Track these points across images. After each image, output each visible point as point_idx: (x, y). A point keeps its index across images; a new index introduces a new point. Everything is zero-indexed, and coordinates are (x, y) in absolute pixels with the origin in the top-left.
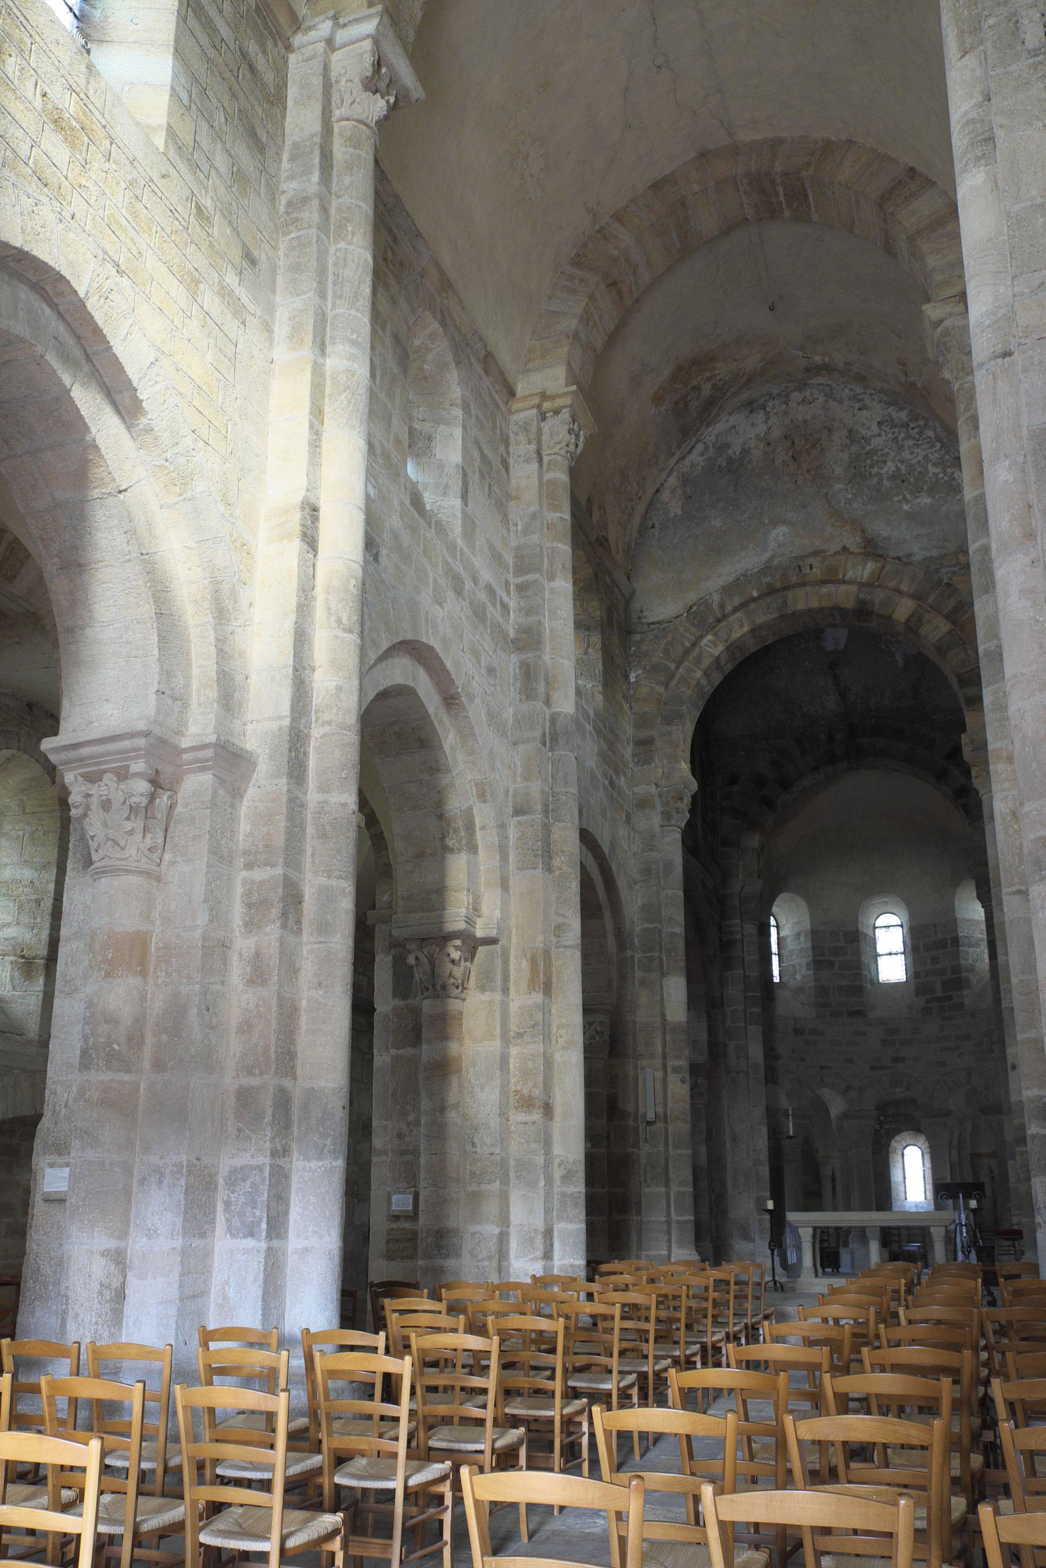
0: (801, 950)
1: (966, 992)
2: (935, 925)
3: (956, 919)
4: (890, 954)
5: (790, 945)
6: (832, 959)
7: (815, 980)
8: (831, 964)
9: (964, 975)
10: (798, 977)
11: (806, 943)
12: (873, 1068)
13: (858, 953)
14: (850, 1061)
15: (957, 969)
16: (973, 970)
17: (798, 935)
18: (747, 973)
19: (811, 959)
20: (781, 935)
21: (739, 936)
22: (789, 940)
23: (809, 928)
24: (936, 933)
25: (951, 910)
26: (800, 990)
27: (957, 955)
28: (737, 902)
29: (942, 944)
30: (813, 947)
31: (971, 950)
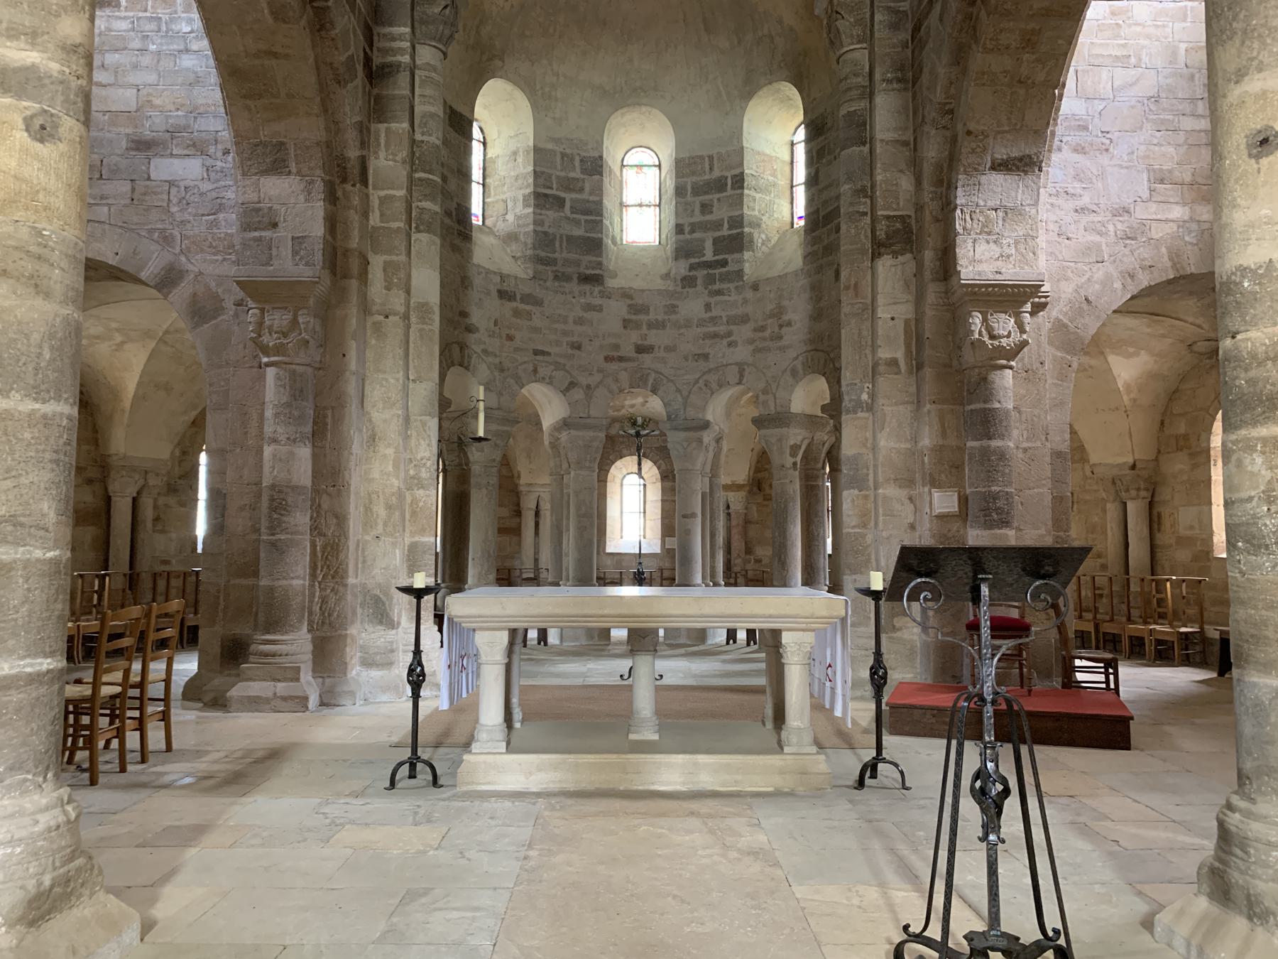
0: (517, 178)
1: (747, 255)
2: (711, 158)
3: (742, 148)
4: (640, 205)
5: (501, 169)
6: (562, 195)
7: (535, 223)
8: (560, 202)
9: (746, 230)
10: (510, 217)
11: (525, 167)
12: (607, 359)
13: (599, 190)
14: (578, 347)
15: (737, 222)
16: (759, 225)
17: (515, 153)
18: (418, 137)
19: (530, 190)
20: (489, 156)
21: (406, 59)
22: (500, 162)
23: (531, 144)
25: (737, 133)
26: (511, 237)
27: (739, 201)
29: (720, 185)
30: (535, 172)
31: (758, 196)
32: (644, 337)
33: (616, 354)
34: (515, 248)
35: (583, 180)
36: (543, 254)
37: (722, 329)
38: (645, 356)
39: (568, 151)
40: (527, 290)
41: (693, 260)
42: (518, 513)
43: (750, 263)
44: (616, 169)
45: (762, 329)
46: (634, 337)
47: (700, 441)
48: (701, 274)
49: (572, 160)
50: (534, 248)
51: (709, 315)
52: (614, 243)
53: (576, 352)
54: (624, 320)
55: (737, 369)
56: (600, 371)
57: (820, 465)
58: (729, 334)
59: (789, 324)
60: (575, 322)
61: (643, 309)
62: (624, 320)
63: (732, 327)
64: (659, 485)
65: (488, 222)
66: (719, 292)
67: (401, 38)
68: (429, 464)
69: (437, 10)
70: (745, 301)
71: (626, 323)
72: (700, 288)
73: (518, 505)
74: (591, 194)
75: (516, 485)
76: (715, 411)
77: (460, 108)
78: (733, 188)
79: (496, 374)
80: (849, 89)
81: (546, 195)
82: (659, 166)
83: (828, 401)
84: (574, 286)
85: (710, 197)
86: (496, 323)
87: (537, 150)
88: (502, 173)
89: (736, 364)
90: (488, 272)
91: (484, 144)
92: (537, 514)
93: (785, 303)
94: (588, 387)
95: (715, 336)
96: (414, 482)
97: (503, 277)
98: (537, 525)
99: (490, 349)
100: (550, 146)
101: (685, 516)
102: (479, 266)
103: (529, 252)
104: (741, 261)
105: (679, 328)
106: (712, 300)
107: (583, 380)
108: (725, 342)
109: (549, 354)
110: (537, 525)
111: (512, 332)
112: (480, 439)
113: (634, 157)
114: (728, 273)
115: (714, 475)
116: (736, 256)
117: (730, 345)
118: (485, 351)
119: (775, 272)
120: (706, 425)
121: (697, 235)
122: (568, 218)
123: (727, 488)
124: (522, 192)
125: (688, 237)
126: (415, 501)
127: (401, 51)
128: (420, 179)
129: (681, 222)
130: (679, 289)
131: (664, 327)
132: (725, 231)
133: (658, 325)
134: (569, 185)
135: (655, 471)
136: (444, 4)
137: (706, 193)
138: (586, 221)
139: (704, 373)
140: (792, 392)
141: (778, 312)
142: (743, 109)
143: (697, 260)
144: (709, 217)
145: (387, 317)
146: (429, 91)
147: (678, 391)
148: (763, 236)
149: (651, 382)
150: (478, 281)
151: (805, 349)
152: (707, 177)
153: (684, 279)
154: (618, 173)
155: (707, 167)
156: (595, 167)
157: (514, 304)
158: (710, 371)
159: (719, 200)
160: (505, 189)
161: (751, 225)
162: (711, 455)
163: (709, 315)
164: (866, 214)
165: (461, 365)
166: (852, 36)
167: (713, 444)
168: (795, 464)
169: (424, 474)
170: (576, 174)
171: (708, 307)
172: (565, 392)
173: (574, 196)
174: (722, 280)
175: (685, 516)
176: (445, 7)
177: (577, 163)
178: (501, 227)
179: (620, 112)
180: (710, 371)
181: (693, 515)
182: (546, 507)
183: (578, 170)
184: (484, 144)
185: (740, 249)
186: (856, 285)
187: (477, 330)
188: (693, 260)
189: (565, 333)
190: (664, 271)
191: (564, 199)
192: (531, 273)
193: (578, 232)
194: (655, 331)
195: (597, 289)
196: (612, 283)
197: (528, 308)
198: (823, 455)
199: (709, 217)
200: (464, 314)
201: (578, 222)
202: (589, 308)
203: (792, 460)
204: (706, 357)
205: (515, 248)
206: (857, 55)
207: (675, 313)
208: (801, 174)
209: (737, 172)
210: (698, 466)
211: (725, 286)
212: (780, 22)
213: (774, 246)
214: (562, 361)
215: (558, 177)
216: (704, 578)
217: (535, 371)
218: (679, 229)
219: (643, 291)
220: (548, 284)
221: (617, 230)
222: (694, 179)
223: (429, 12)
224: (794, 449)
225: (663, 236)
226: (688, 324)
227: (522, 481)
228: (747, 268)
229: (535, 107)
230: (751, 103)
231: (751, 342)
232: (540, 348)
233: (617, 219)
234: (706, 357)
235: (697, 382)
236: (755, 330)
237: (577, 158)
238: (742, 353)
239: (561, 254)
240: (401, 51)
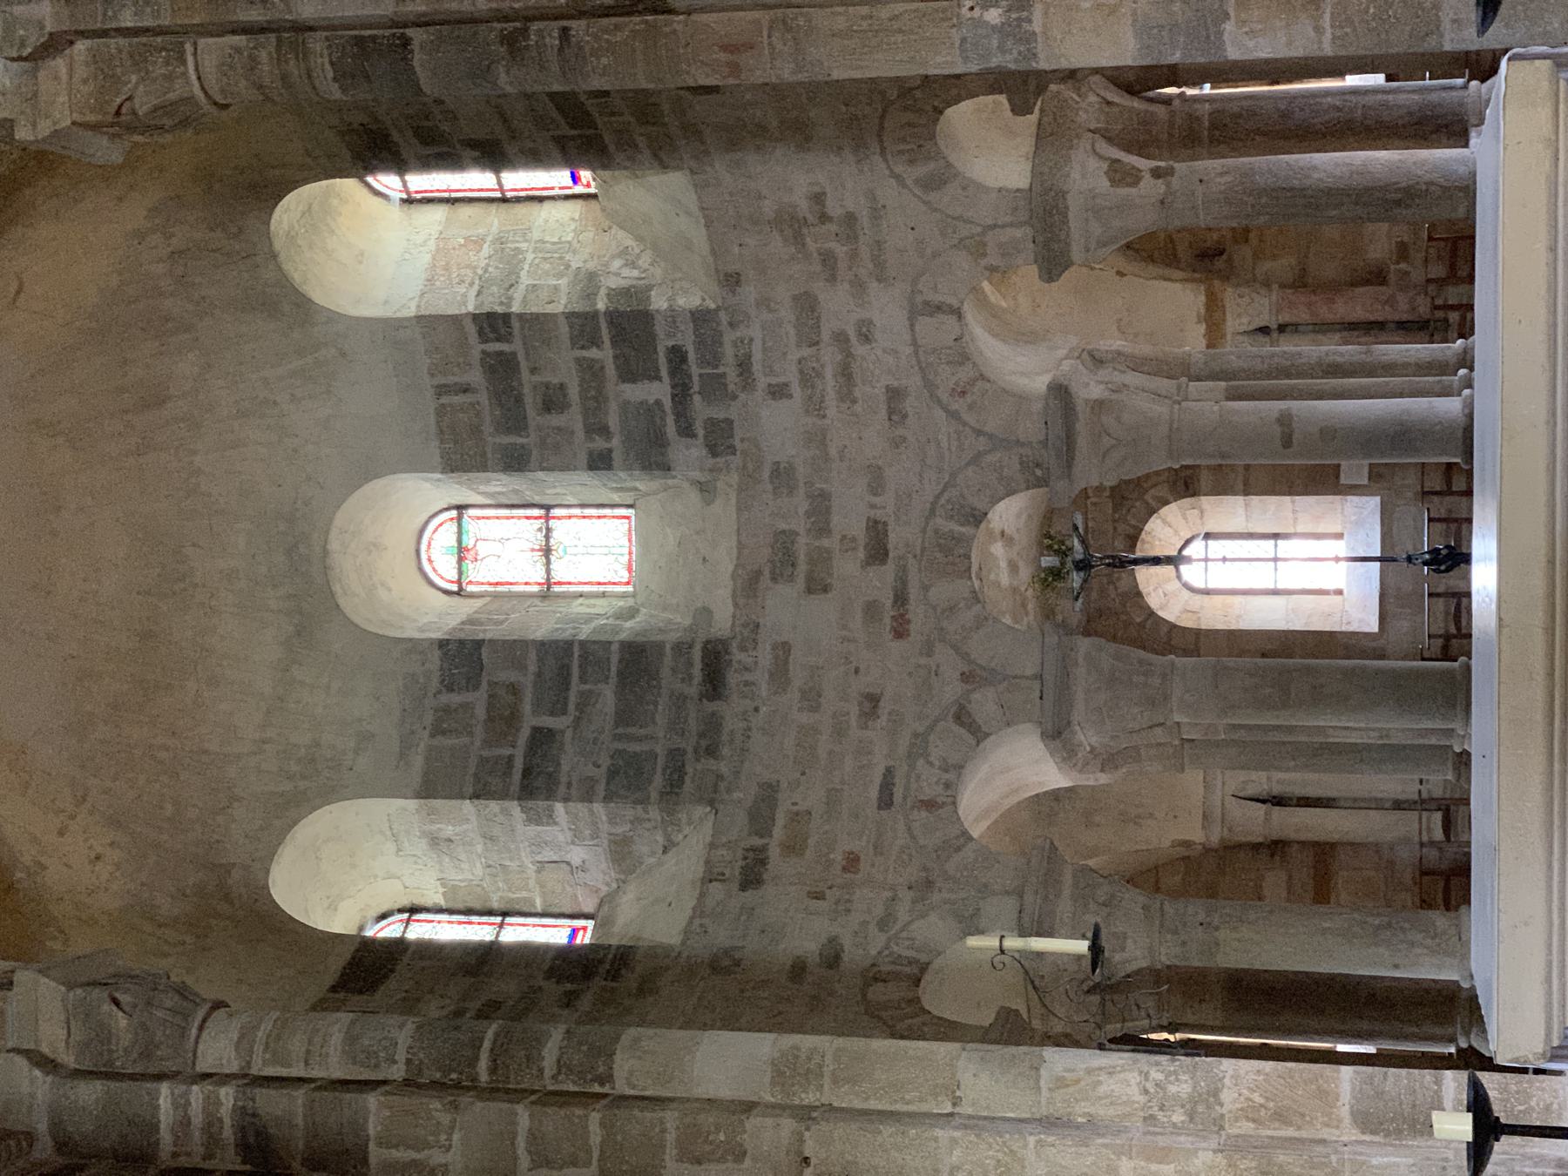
1: (659, 302)
2: (441, 390)
4: (547, 551)
5: (470, 872)
6: (525, 733)
7: (588, 797)
9: (601, 305)
10: (577, 855)
12: (900, 633)
13: (514, 650)
14: (872, 702)
15: (583, 326)
16: (592, 276)
17: (435, 841)
18: (397, 1072)
19: (514, 807)
20: (438, 899)
21: (227, 1096)
23: (412, 804)
24: (466, 389)
25: (389, 329)
26: (621, 853)
27: (537, 322)
28: (89, 1093)
29: (502, 369)
30: (476, 796)
31: (525, 280)
32: (848, 542)
33: (889, 612)
34: (646, 845)
35: (492, 684)
36: (659, 780)
37: (830, 357)
38: (893, 538)
39: (429, 718)
40: (742, 819)
41: (671, 429)
42: (1276, 848)
43: (679, 295)
44: (465, 608)
45: (828, 259)
46: (848, 566)
47: (1099, 405)
48: (701, 410)
49: (447, 710)
50: (645, 801)
51: (796, 390)
52: (632, 613)
53: (885, 706)
54: (809, 591)
56: (929, 651)
57: (1160, 110)
58: (841, 338)
59: (818, 198)
60: (815, 709)
61: (784, 545)
62: (809, 591)
63: (826, 336)
64: (1205, 501)
65: (589, 908)
66: (744, 365)
67: (181, 1105)
68: (1156, 1075)
69: (122, 1021)
70: (764, 303)
71: (817, 586)
72: (733, 411)
73: (1256, 847)
74: (523, 668)
75: (1207, 850)
76: (1025, 370)
77: (335, 965)
78: (507, 338)
79: (936, 897)
80: (284, 77)
81: (527, 772)
82: (460, 508)
83: (1003, 98)
84: (731, 711)
85: (526, 390)
86: (819, 896)
87: (427, 791)
88: (479, 871)
90: (699, 911)
91: (413, 910)
92: (1279, 801)
93: (768, 208)
94: (966, 677)
95: (846, 374)
96: (1203, 1113)
97: (711, 876)
98: (1306, 802)
99: (879, 911)
100: (418, 762)
101: (1287, 442)
102: (687, 932)
103: (654, 813)
104: (673, 315)
105: (827, 458)
106: (762, 381)
107: (951, 690)
108: (860, 350)
109: (889, 772)
110: (1306, 802)
111: (838, 857)
112: (1096, 949)
113: (443, 567)
114: (700, 343)
115: (1181, 370)
116: (660, 329)
117: (866, 338)
118: (883, 925)
119: (698, 235)
120: (1060, 391)
121: (613, 421)
122: (578, 720)
123: (1214, 334)
124: (520, 827)
125: (615, 442)
126: (1250, 1113)
127: (211, 1103)
128: (493, 1070)
129: (583, 458)
130: (736, 460)
131: (824, 496)
132: (604, 354)
133: (820, 508)
134: (503, 719)
135: (1171, 511)
136: (108, 1007)
137: (519, 400)
138: (583, 680)
140: (981, 188)
141: (792, 225)
142: (334, 317)
143: (670, 420)
144: (574, 392)
145: (806, 1160)
146: (297, 1045)
147: (976, 459)
148: (617, 264)
150: (721, 936)
151: (877, 158)
152: (483, 398)
153: (713, 451)
154: (478, 603)
155: (458, 399)
156: (463, 657)
157: (774, 852)
158: (930, 386)
159: (533, 371)
160: (513, 865)
161: (590, 296)
162: (1132, 379)
163: (796, 390)
164: (565, 30)
165: (917, 982)
166: (169, 78)
167: (1104, 374)
168: (1157, 173)
169: (1182, 1088)
170: (478, 699)
171: (778, 392)
172: (979, 735)
173: (527, 708)
174: (715, 359)
175: (1287, 442)
176: (116, 1002)
177: (456, 699)
178: (600, 875)
179: (341, 602)
180: (930, 386)
181: (1285, 420)
182: (1262, 781)
183: (468, 697)
184: (413, 910)
185: (644, 318)
186: (725, 48)
187: (833, 940)
188: (671, 429)
189: (840, 732)
190: (694, 496)
191: (536, 730)
192: (701, 810)
193: (608, 697)
194: (835, 520)
195: (737, 656)
196: (723, 620)
197: (781, 819)
198: (1136, 104)
199: (574, 392)
200: (798, 970)
201: (586, 700)
202: (780, 674)
203: (1147, 182)
205: (646, 845)
206: (210, 64)
207: (791, 469)
208: (477, 180)
209: (472, 330)
210: (1160, 409)
211: (729, 351)
212: (140, 236)
213: (640, 239)
214: (904, 742)
215: (487, 743)
216: (1446, 392)
217: (930, 805)
218: (599, 462)
219: (741, 546)
220: (724, 768)
221: (601, 606)
222: (487, 428)
223: (126, 1039)
224: (1120, 175)
225: (616, 498)
226: (817, 439)
227: (1197, 836)
228: (689, 300)
229: (331, 793)
230: (318, 297)
231: (859, 286)
232: (874, 793)
233: (578, 608)
234: (895, 395)
235: (954, 415)
236: (832, 279)
237: (445, 698)
238: (886, 309)
239: (657, 737)
240: (211, 1103)
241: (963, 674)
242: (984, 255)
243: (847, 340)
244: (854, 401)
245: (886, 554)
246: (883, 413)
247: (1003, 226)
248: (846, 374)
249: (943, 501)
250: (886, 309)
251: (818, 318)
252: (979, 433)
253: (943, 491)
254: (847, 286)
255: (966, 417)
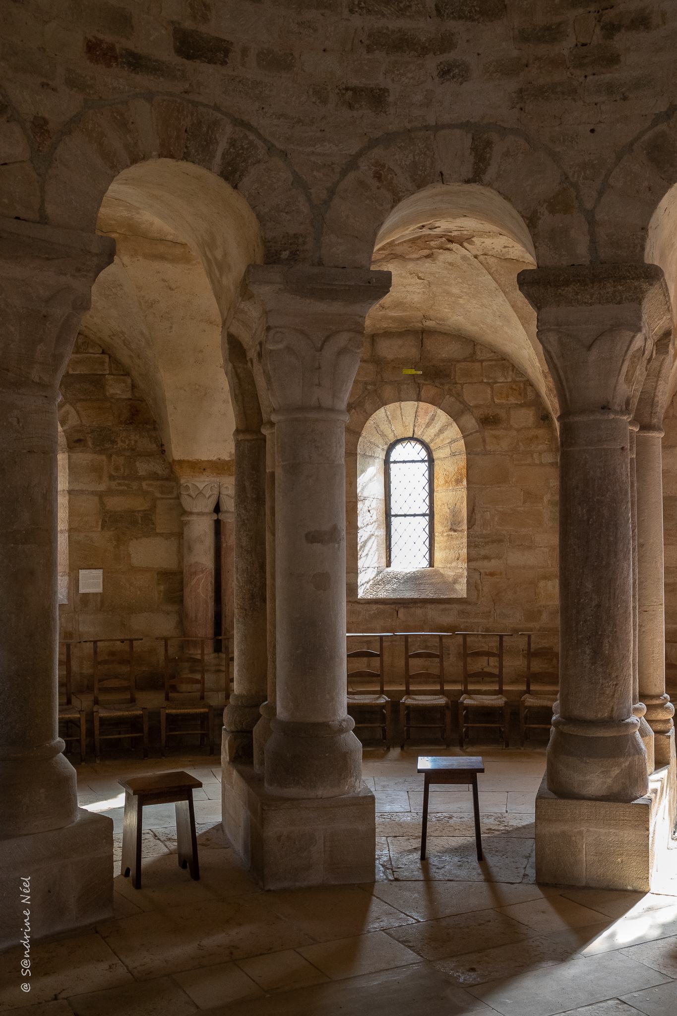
45: (551, 33)
55: (468, 142)
89: (465, 126)
95: (402, 43)
108: (432, 63)
117: (445, 72)
139: (373, 143)
149: (222, 146)
158: (389, 139)
180: (389, 139)
204: (377, 98)
234: (377, 98)
235: (352, 164)
238: (484, 98)
241: (46, 122)
242: (553, 211)
243: (443, 51)
244: (369, 50)
245: (189, 57)
246: (355, 82)
247: (592, 234)
248: (402, 43)
249: (252, 137)
250: (484, 98)
251: (471, 19)
252: (332, 192)
253: (260, 137)
254: (515, 53)
255: (351, 176)
